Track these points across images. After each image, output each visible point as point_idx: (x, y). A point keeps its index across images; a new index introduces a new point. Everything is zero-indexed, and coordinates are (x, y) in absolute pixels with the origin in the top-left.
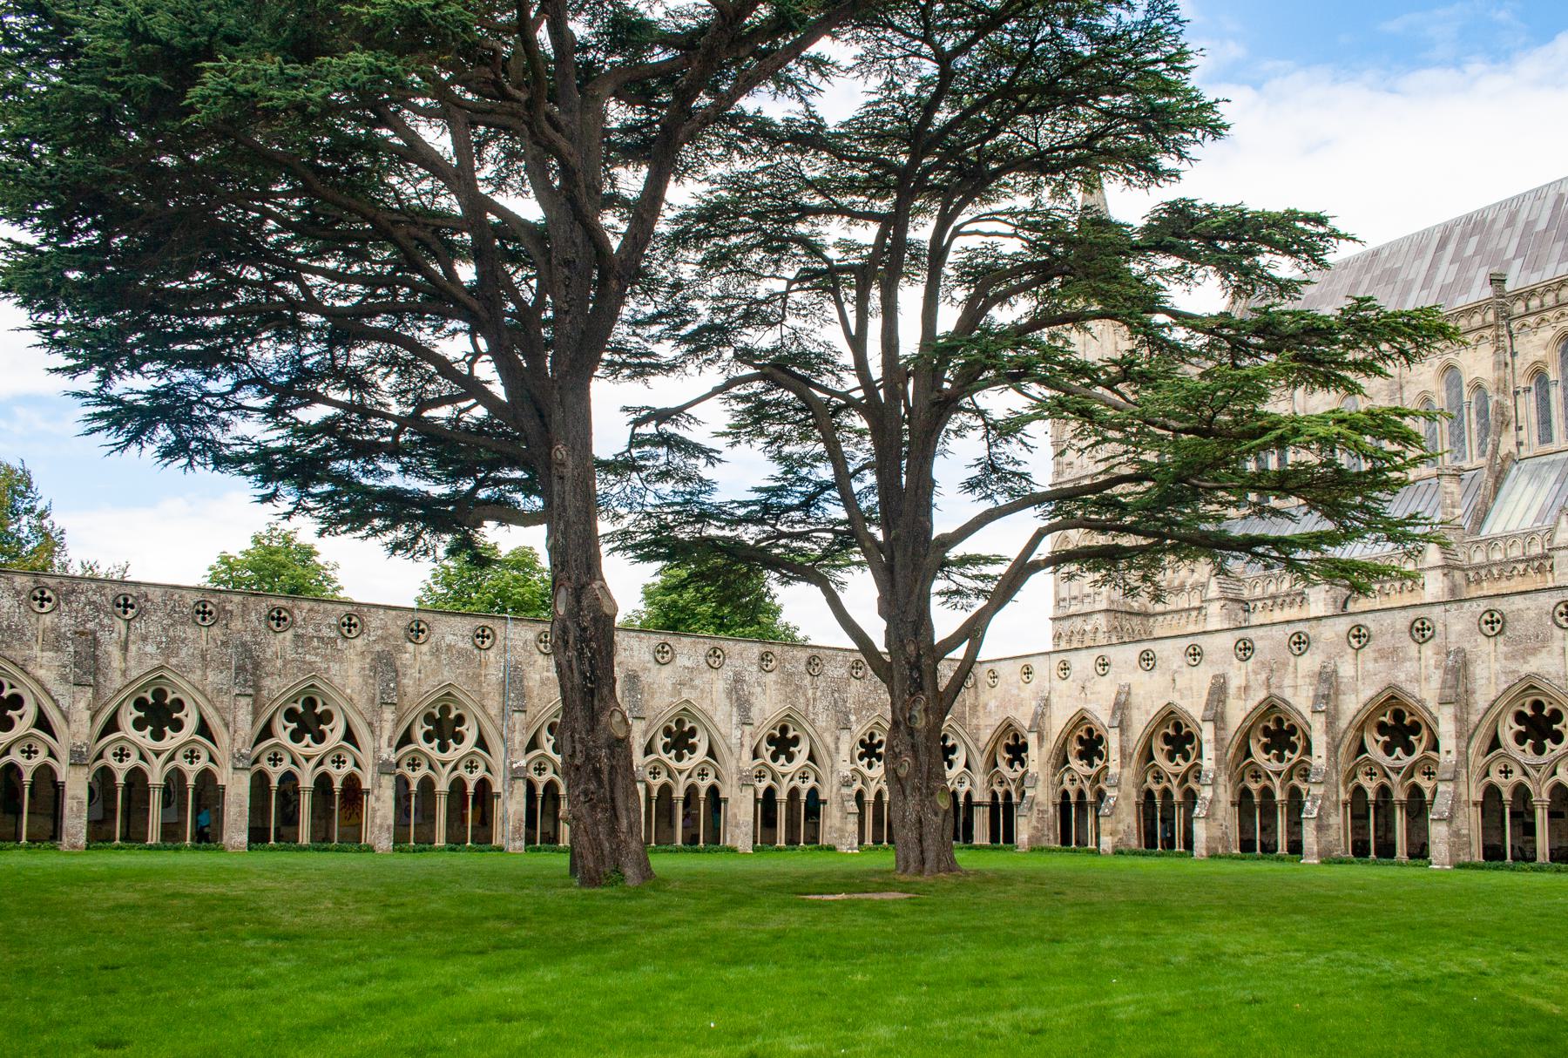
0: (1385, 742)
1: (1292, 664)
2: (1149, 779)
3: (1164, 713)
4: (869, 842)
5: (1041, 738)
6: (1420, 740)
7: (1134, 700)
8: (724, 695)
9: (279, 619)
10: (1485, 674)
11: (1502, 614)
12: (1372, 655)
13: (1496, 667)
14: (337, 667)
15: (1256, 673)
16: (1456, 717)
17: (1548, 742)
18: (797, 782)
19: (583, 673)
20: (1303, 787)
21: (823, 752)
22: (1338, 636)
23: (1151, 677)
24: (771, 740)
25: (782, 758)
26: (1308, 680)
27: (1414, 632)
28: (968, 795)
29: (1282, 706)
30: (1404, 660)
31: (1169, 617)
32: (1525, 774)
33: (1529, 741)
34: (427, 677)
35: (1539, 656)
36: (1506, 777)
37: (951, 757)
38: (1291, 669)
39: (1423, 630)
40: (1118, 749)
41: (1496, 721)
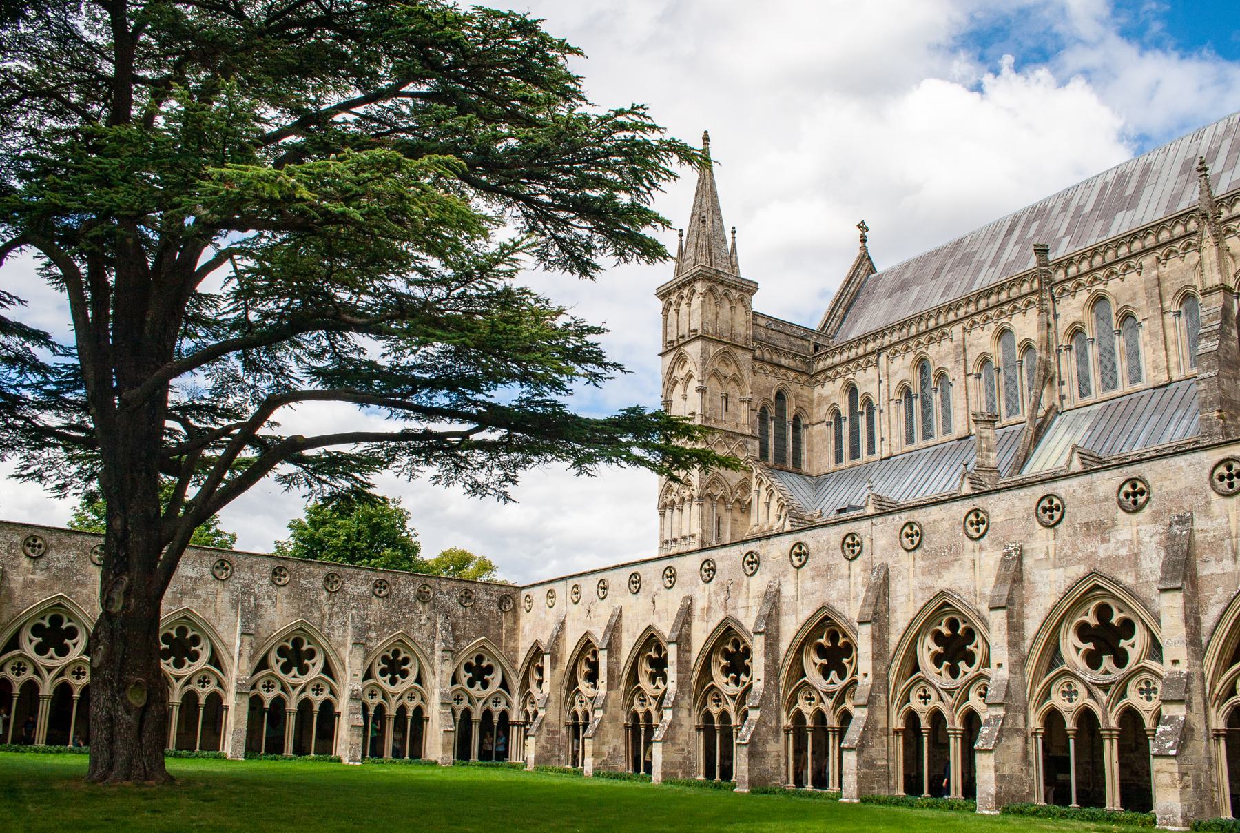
0: (821, 664)
1: (745, 584)
3: (647, 636)
5: (554, 661)
7: (625, 622)
8: (229, 606)
10: (906, 591)
11: (920, 526)
12: (810, 574)
13: (914, 583)
15: (717, 594)
16: (873, 636)
18: (309, 694)
22: (782, 554)
23: (637, 599)
26: (757, 600)
29: (736, 628)
30: (837, 577)
33: (946, 663)
35: (952, 570)
36: (925, 703)
37: (486, 677)
38: (744, 589)
39: (853, 546)
40: (605, 671)
41: (914, 642)
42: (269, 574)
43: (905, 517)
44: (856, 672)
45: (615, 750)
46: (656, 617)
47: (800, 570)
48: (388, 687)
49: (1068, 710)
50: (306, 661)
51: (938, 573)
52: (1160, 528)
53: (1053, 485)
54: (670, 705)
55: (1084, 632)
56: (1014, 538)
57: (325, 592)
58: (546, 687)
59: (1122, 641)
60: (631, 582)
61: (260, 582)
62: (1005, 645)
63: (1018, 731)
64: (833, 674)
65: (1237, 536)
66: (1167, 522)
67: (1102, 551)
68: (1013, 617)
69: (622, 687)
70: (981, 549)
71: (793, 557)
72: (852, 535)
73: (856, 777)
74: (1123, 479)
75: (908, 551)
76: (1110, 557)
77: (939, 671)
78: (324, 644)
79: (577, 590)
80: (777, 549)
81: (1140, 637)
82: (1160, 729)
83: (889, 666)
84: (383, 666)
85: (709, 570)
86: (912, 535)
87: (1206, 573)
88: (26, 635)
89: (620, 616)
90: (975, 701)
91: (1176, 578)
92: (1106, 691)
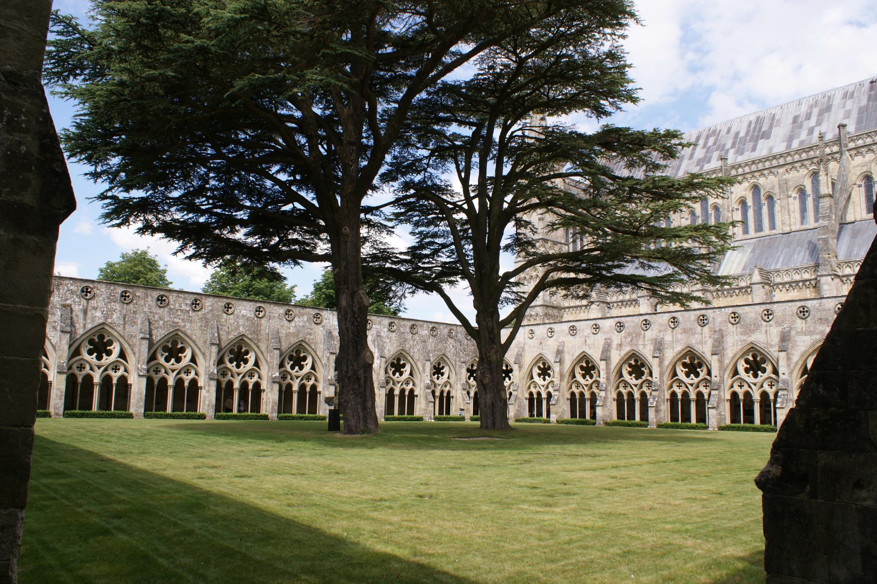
5: (520, 367)
6: (702, 371)
7: (566, 349)
9: (162, 300)
13: (736, 338)
14: (189, 325)
15: (625, 338)
17: (759, 373)
19: (353, 333)
20: (648, 392)
24: (393, 365)
25: (397, 374)
30: (695, 333)
31: (571, 309)
32: (750, 387)
34: (232, 330)
38: (642, 336)
42: (387, 325)
46: (587, 347)
70: (770, 326)
74: (838, 302)
75: (733, 324)
88: (160, 351)
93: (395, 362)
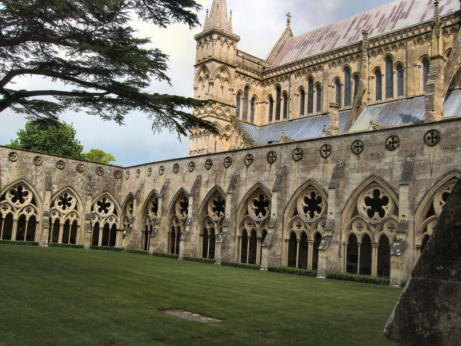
1: (224, 172)
2: (174, 222)
3: (180, 192)
4: (60, 241)
7: (170, 186)
11: (302, 150)
12: (253, 168)
13: (298, 175)
16: (278, 198)
18: (25, 212)
21: (38, 199)
23: (177, 176)
27: (269, 158)
28: (114, 226)
29: (219, 191)
33: (309, 211)
36: (299, 229)
37: (107, 208)
38: (224, 174)
41: (296, 201)
43: (295, 146)
44: (270, 213)
45: (163, 243)
46: (185, 184)
47: (249, 166)
48: (61, 210)
49: (359, 234)
50: (24, 197)
51: (308, 171)
52: (402, 158)
53: (360, 136)
54: (188, 224)
55: (368, 201)
56: (341, 158)
57: (34, 166)
58: (134, 214)
59: (383, 206)
60: (174, 168)
61: (3, 159)
62: (334, 204)
63: (337, 242)
64: (260, 214)
65: (433, 164)
66: (405, 156)
67: (378, 167)
68: (338, 193)
69: (168, 215)
70: (327, 162)
71: (246, 160)
72: (272, 152)
73: (267, 259)
75: (296, 161)
76: (380, 169)
77: (306, 215)
78: (33, 189)
79: (150, 170)
80: (240, 157)
81: (390, 205)
82: (395, 244)
83: (284, 211)
84: (59, 201)
85: (209, 164)
86: (298, 154)
87: (419, 179)
89: (169, 183)
90: (320, 228)
91: (407, 180)
92: (375, 227)
93: (102, 201)
